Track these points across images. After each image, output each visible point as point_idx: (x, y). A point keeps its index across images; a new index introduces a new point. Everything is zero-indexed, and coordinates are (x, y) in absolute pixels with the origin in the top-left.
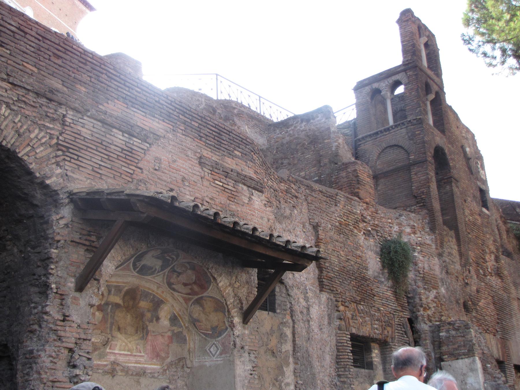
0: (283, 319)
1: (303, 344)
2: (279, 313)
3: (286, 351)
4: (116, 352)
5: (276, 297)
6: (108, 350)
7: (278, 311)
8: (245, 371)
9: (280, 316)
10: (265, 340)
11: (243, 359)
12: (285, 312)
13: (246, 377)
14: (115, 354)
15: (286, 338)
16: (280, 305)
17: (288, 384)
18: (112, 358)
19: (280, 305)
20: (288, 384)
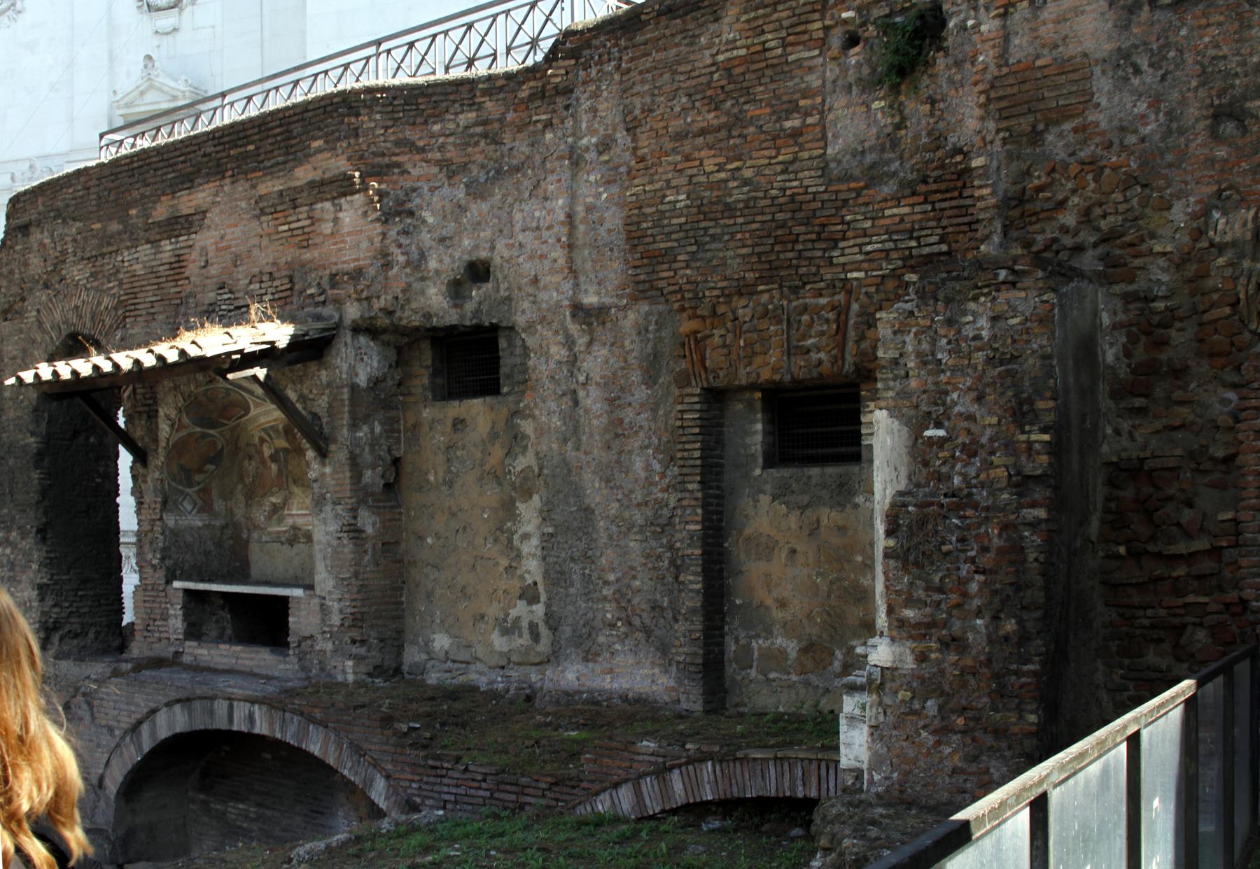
0: (518, 403)
1: (551, 448)
2: (508, 394)
3: (522, 471)
4: (294, 512)
5: (501, 362)
6: (286, 512)
7: (505, 390)
8: (327, 533)
9: (511, 399)
10: (479, 455)
11: (323, 515)
12: (522, 388)
13: (329, 544)
14: (292, 515)
15: (525, 443)
16: (509, 376)
17: (526, 536)
18: (290, 521)
19: (509, 376)
20: (526, 536)
